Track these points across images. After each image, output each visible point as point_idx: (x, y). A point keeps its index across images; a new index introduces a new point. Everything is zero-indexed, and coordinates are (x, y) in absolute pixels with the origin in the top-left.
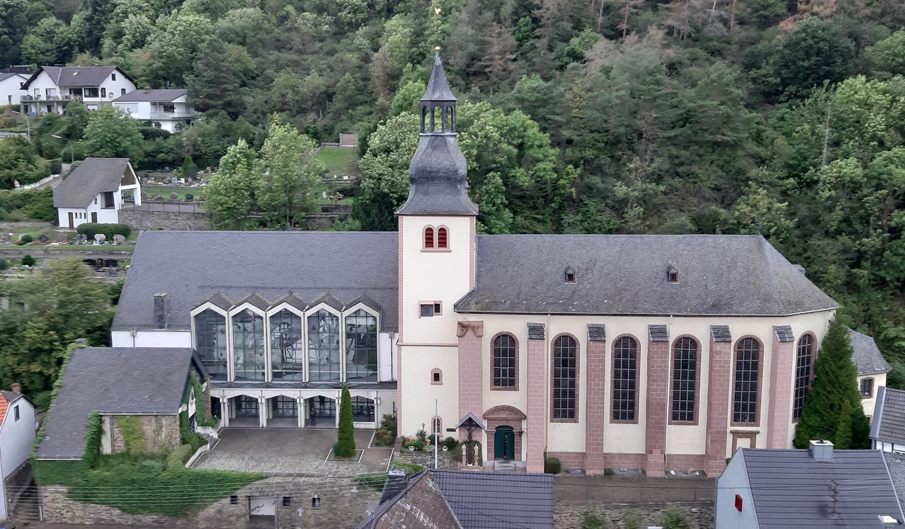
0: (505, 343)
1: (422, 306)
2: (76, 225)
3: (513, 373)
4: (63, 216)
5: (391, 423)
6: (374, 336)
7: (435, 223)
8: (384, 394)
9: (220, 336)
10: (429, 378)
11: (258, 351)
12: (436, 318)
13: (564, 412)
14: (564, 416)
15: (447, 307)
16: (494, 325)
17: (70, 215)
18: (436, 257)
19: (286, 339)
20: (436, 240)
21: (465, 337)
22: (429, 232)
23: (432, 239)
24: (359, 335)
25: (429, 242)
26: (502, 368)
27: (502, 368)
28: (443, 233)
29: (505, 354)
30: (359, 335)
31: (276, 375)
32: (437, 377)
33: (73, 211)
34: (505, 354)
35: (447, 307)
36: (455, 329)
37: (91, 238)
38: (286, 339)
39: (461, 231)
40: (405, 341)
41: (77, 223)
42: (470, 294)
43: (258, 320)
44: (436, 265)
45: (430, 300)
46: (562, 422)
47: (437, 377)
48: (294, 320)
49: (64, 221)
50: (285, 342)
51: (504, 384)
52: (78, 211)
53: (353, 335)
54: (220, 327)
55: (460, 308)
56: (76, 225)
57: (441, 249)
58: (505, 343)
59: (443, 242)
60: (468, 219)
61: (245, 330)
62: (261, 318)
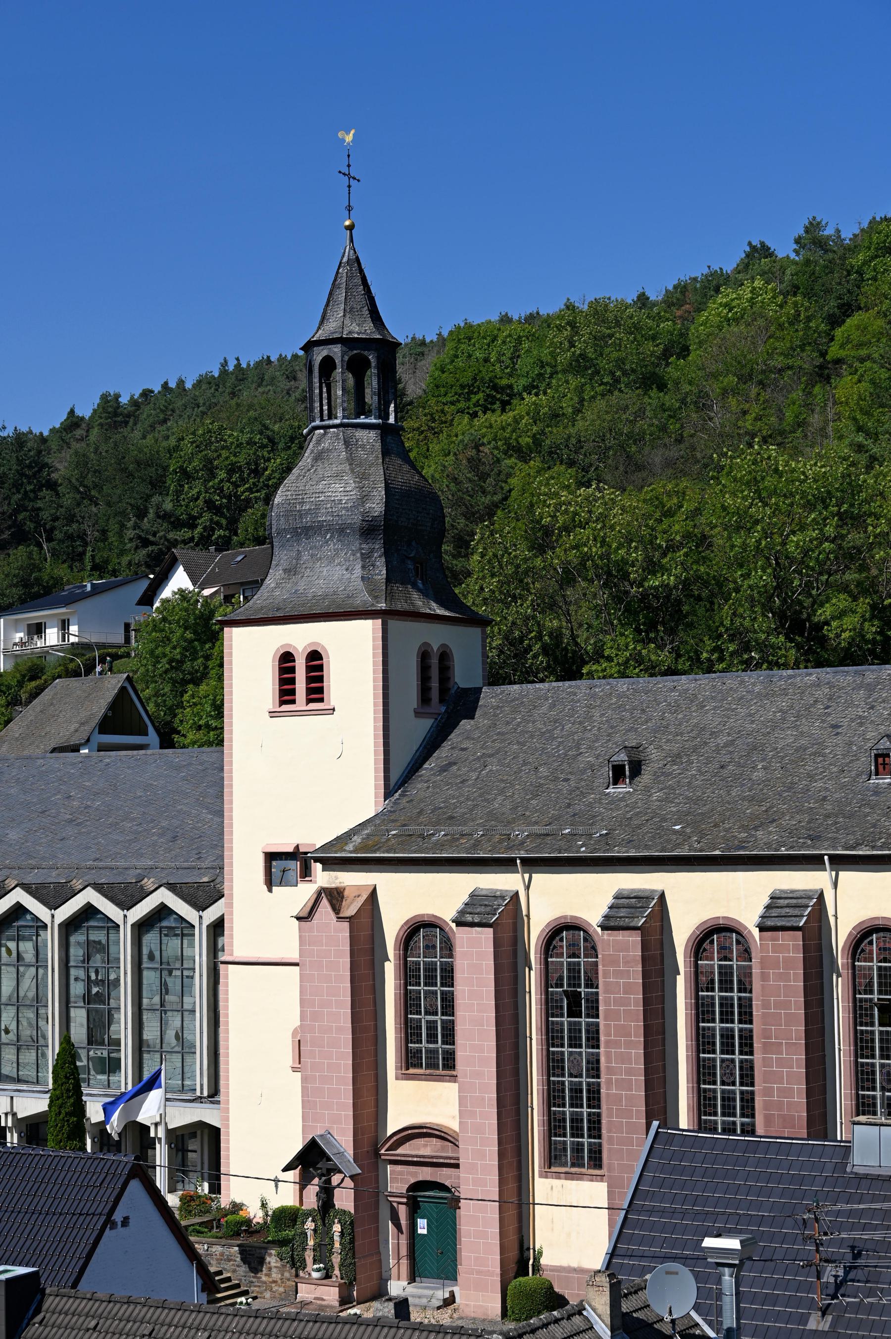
7: (300, 637)
13: (578, 1149)
14: (577, 1162)
16: (404, 897)
18: (303, 727)
19: (97, 983)
20: (302, 682)
22: (286, 659)
26: (424, 1018)
27: (424, 1018)
28: (315, 658)
38: (97, 983)
39: (353, 651)
44: (302, 751)
46: (569, 1176)
50: (95, 990)
51: (432, 1065)
57: (313, 706)
60: (369, 622)
61: (19, 957)
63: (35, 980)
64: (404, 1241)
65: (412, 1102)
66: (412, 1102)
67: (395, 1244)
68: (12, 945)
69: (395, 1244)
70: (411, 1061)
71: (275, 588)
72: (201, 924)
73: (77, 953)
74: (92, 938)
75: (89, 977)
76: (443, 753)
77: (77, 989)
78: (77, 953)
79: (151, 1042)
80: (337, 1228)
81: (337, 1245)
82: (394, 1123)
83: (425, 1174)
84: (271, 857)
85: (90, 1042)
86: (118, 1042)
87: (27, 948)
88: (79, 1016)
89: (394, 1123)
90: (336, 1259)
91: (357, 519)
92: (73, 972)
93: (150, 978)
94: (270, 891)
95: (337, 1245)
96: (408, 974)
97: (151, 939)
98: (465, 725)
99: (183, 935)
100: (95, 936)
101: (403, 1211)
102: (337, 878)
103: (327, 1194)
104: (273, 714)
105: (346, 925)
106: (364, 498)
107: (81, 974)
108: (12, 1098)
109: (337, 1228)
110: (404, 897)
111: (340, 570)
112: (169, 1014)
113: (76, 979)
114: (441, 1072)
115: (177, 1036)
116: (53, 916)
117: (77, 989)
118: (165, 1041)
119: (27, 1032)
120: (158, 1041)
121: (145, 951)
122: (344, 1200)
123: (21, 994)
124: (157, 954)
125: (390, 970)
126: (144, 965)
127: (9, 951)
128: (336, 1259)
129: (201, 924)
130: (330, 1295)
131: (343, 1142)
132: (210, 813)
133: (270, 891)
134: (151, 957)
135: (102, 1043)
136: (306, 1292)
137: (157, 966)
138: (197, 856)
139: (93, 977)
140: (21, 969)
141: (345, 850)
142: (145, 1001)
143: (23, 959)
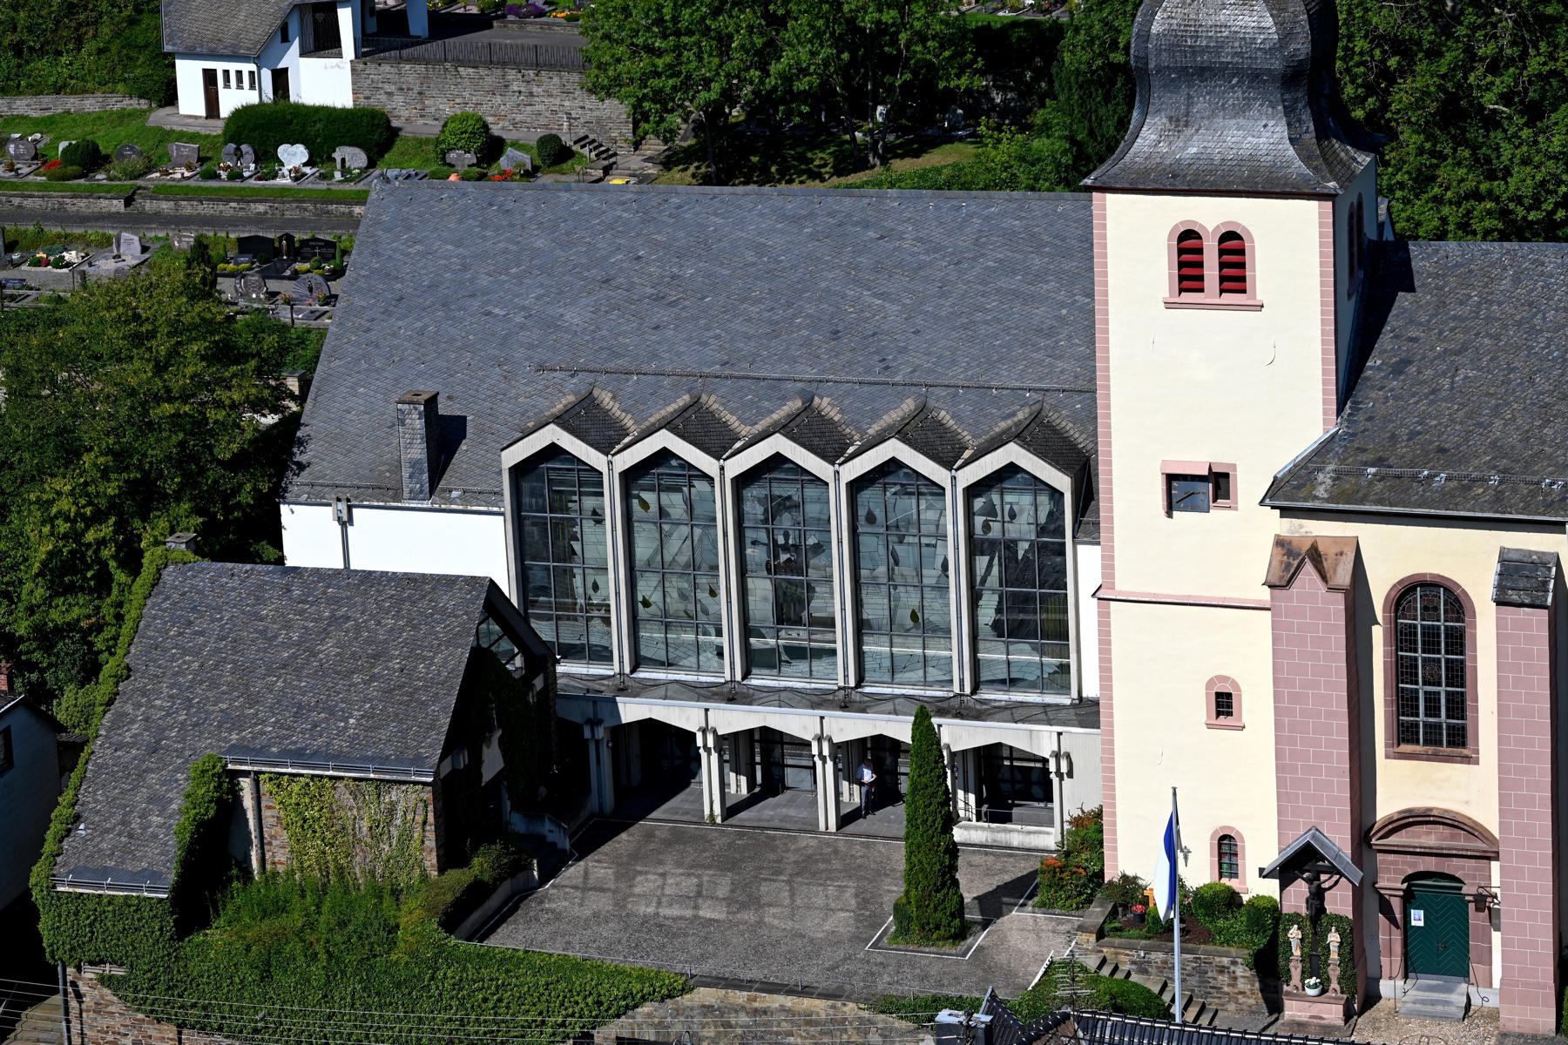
0: (1430, 610)
1: (1171, 478)
2: (225, 110)
3: (1459, 706)
4: (189, 75)
5: (1090, 832)
6: (1061, 552)
7: (1211, 214)
8: (1077, 739)
9: (588, 525)
10: (1201, 706)
11: (702, 581)
12: (1217, 516)
15: (1251, 485)
16: (1394, 554)
17: (209, 76)
18: (1212, 323)
19: (786, 548)
20: (1212, 269)
21: (1295, 588)
22: (1188, 242)
23: (1200, 265)
24: (1011, 545)
25: (1189, 276)
26: (1422, 689)
27: (1422, 689)
28: (1233, 245)
29: (1431, 644)
30: (1011, 545)
31: (753, 660)
32: (1224, 704)
33: (219, 66)
34: (1431, 644)
35: (1251, 485)
36: (1258, 561)
37: (267, 159)
38: (786, 548)
39: (1292, 243)
40: (1123, 585)
41: (231, 100)
42: (1321, 452)
43: (700, 486)
45: (1196, 461)
47: (1224, 704)
48: (811, 491)
49: (191, 100)
50: (784, 557)
51: (1433, 737)
52: (233, 67)
53: (993, 544)
54: (589, 503)
55: (1287, 494)
56: (225, 110)
57: (1229, 298)
58: (1430, 610)
59: (1235, 277)
60: (1312, 206)
61: (662, 512)
62: (710, 479)
63: (689, 542)
64: (1397, 936)
65: (1404, 784)
66: (1404, 784)
67: (1388, 939)
68: (649, 497)
69: (1388, 939)
70: (1404, 734)
71: (1150, 139)
72: (954, 485)
73: (754, 510)
74: (776, 492)
75: (775, 541)
76: (1385, 341)
77: (755, 554)
78: (754, 510)
79: (874, 623)
80: (1334, 938)
81: (1334, 956)
82: (1387, 805)
83: (1430, 864)
84: (1171, 478)
85: (780, 621)
86: (829, 623)
87: (675, 503)
88: (762, 588)
89: (1387, 805)
90: (1334, 972)
91: (1277, 64)
92: (750, 535)
93: (867, 543)
94: (1169, 515)
95: (1334, 956)
96: (1401, 638)
97: (870, 498)
98: (1403, 300)
99: (920, 494)
100: (780, 490)
101: (1396, 904)
102: (1301, 527)
103: (1317, 896)
104: (1169, 305)
105: (1340, 597)
106: (1286, 36)
107: (762, 537)
108: (707, 710)
109: (1334, 938)
110: (1394, 554)
111: (1264, 135)
112: (901, 589)
113: (754, 543)
114: (1445, 749)
115: (914, 616)
116: (722, 468)
117: (755, 554)
118: (897, 620)
119: (675, 604)
120: (886, 621)
121: (862, 513)
122: (1339, 901)
123: (668, 558)
124: (879, 513)
125: (1378, 634)
126: (860, 530)
127: (645, 505)
128: (1334, 972)
129: (954, 485)
130: (1332, 1013)
131: (1339, 840)
132: (875, 295)
133: (1169, 515)
134: (871, 519)
135: (799, 622)
136: (1293, 1010)
137: (883, 530)
138: (882, 365)
139: (781, 540)
140: (666, 527)
141: (1316, 498)
142: (863, 572)
143: (668, 515)
